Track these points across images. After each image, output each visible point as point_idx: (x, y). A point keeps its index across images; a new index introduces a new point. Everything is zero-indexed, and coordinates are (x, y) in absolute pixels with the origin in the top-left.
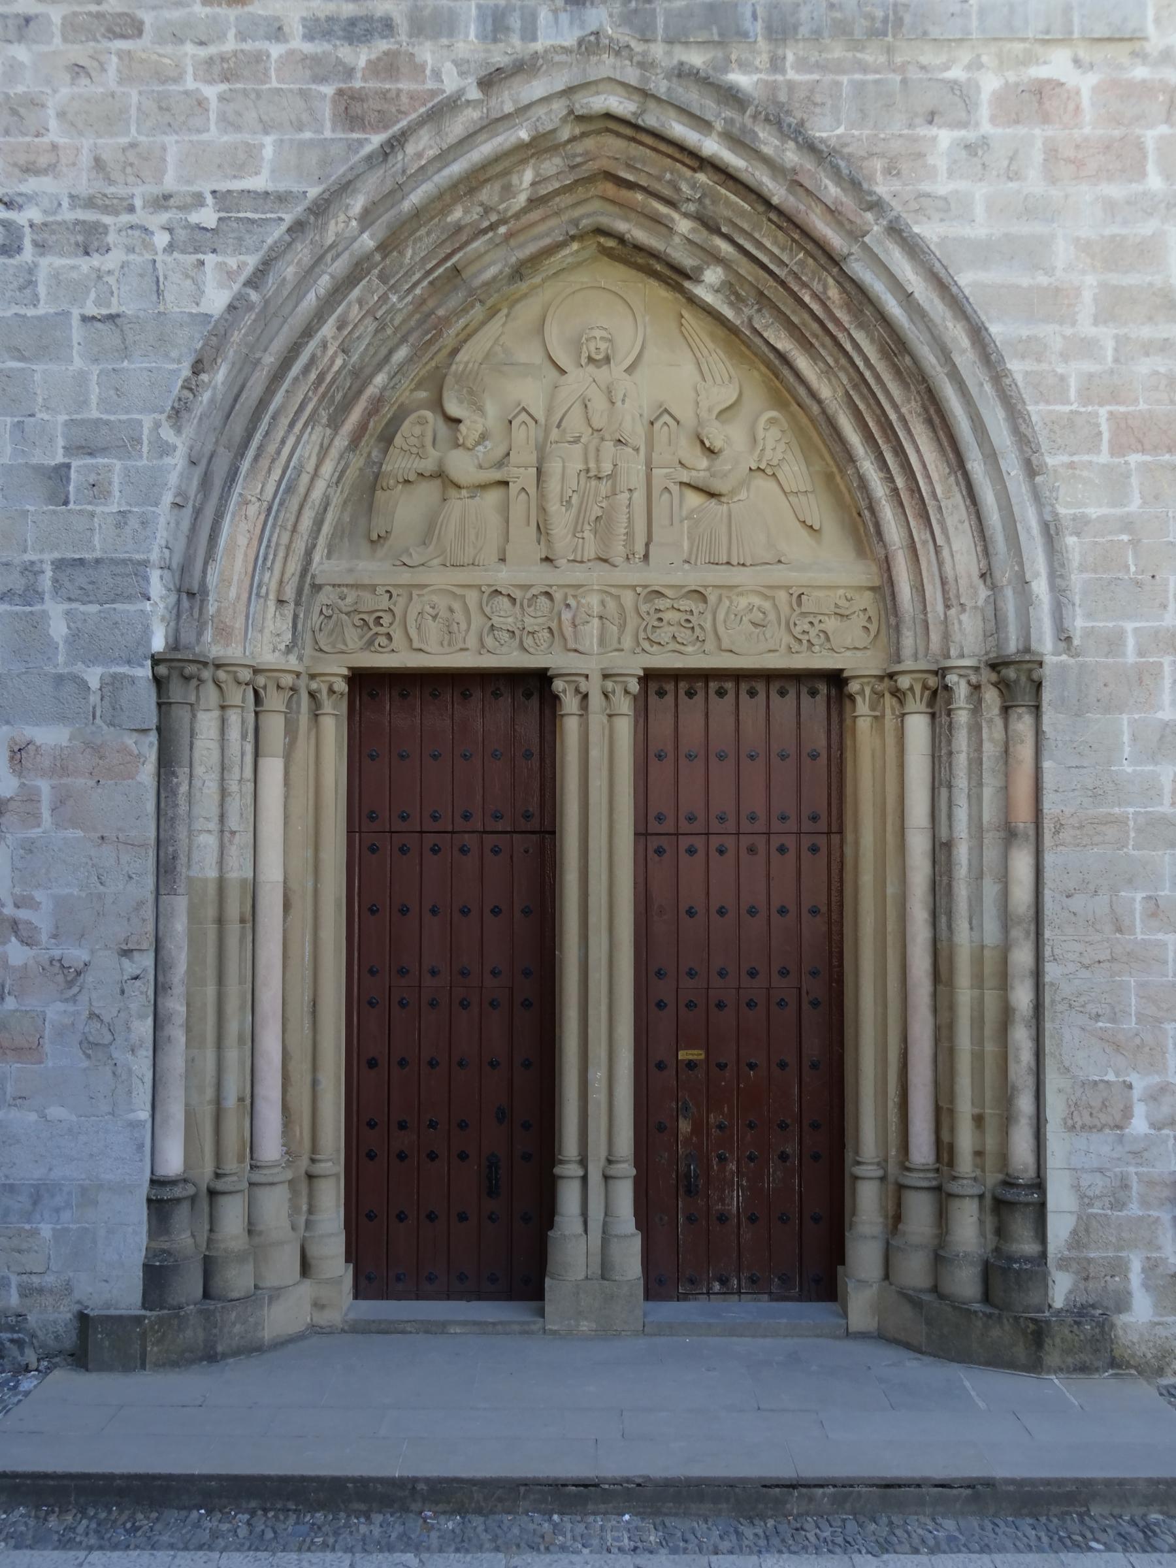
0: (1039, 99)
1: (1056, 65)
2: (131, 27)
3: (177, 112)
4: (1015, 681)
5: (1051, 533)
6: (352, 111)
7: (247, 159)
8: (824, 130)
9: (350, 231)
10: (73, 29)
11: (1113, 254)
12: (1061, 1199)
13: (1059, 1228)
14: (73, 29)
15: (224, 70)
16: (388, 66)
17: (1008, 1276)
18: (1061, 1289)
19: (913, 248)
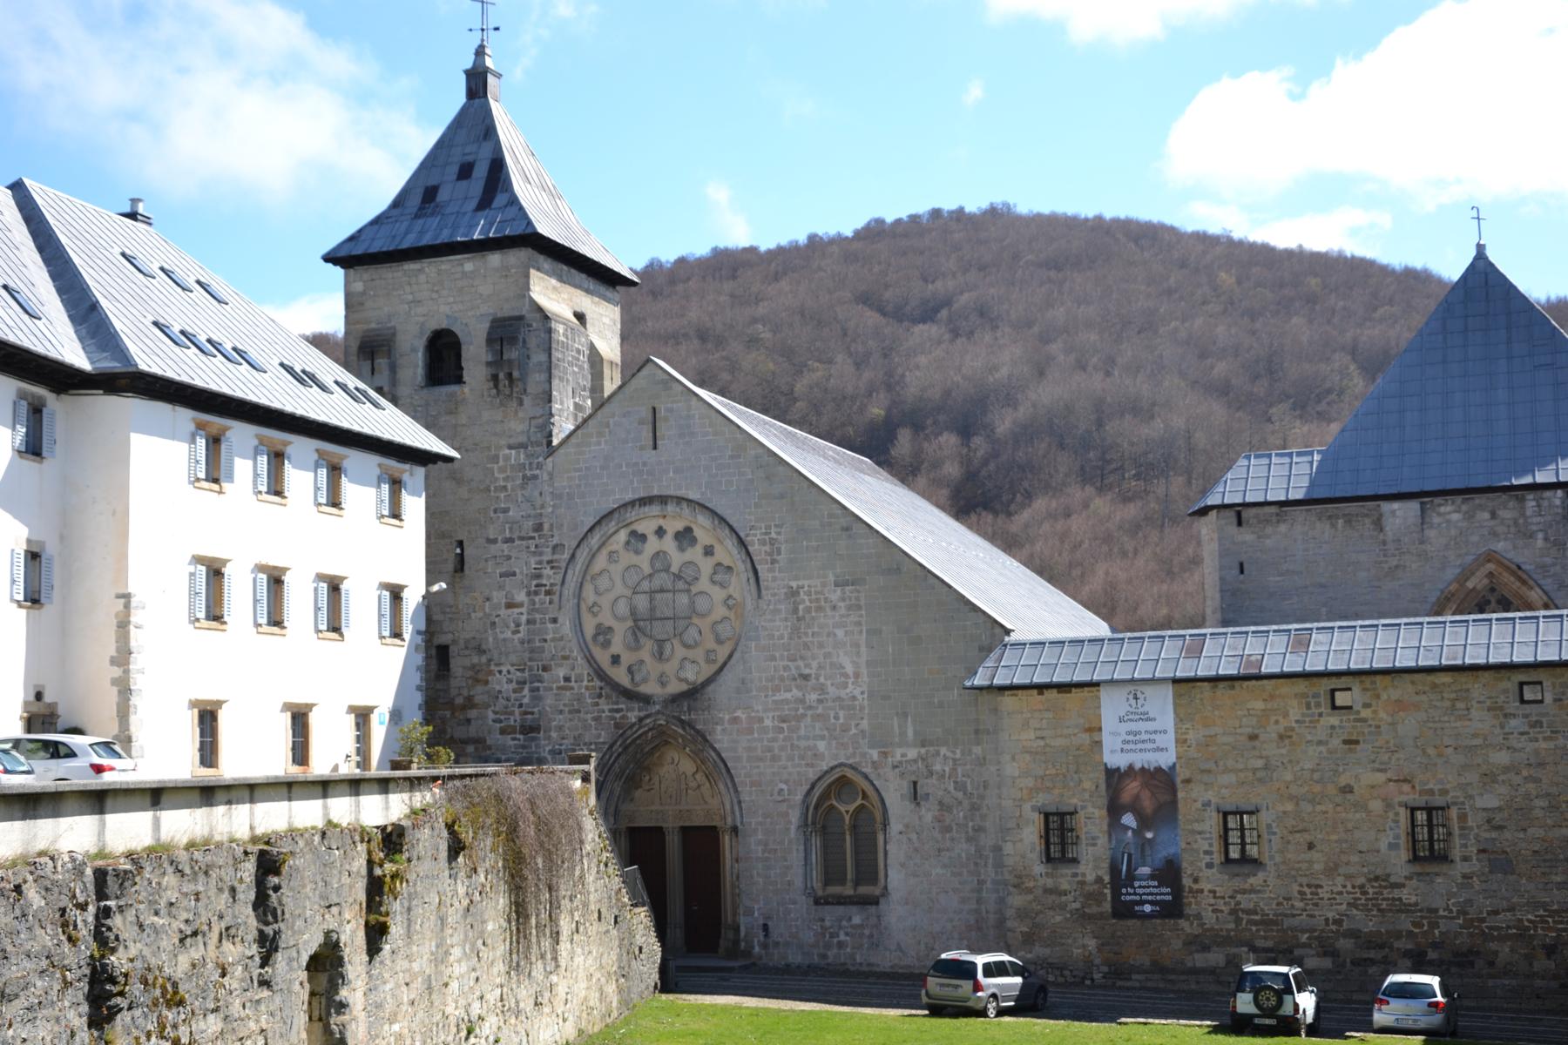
0: (735, 720)
1: (738, 713)
2: (579, 711)
3: (586, 727)
4: (735, 830)
5: (740, 802)
6: (617, 726)
7: (599, 736)
8: (699, 727)
9: (617, 748)
10: (570, 712)
11: (749, 749)
12: (742, 929)
13: (742, 934)
14: (570, 712)
15: (595, 719)
16: (623, 717)
17: (736, 942)
18: (743, 944)
19: (715, 750)
